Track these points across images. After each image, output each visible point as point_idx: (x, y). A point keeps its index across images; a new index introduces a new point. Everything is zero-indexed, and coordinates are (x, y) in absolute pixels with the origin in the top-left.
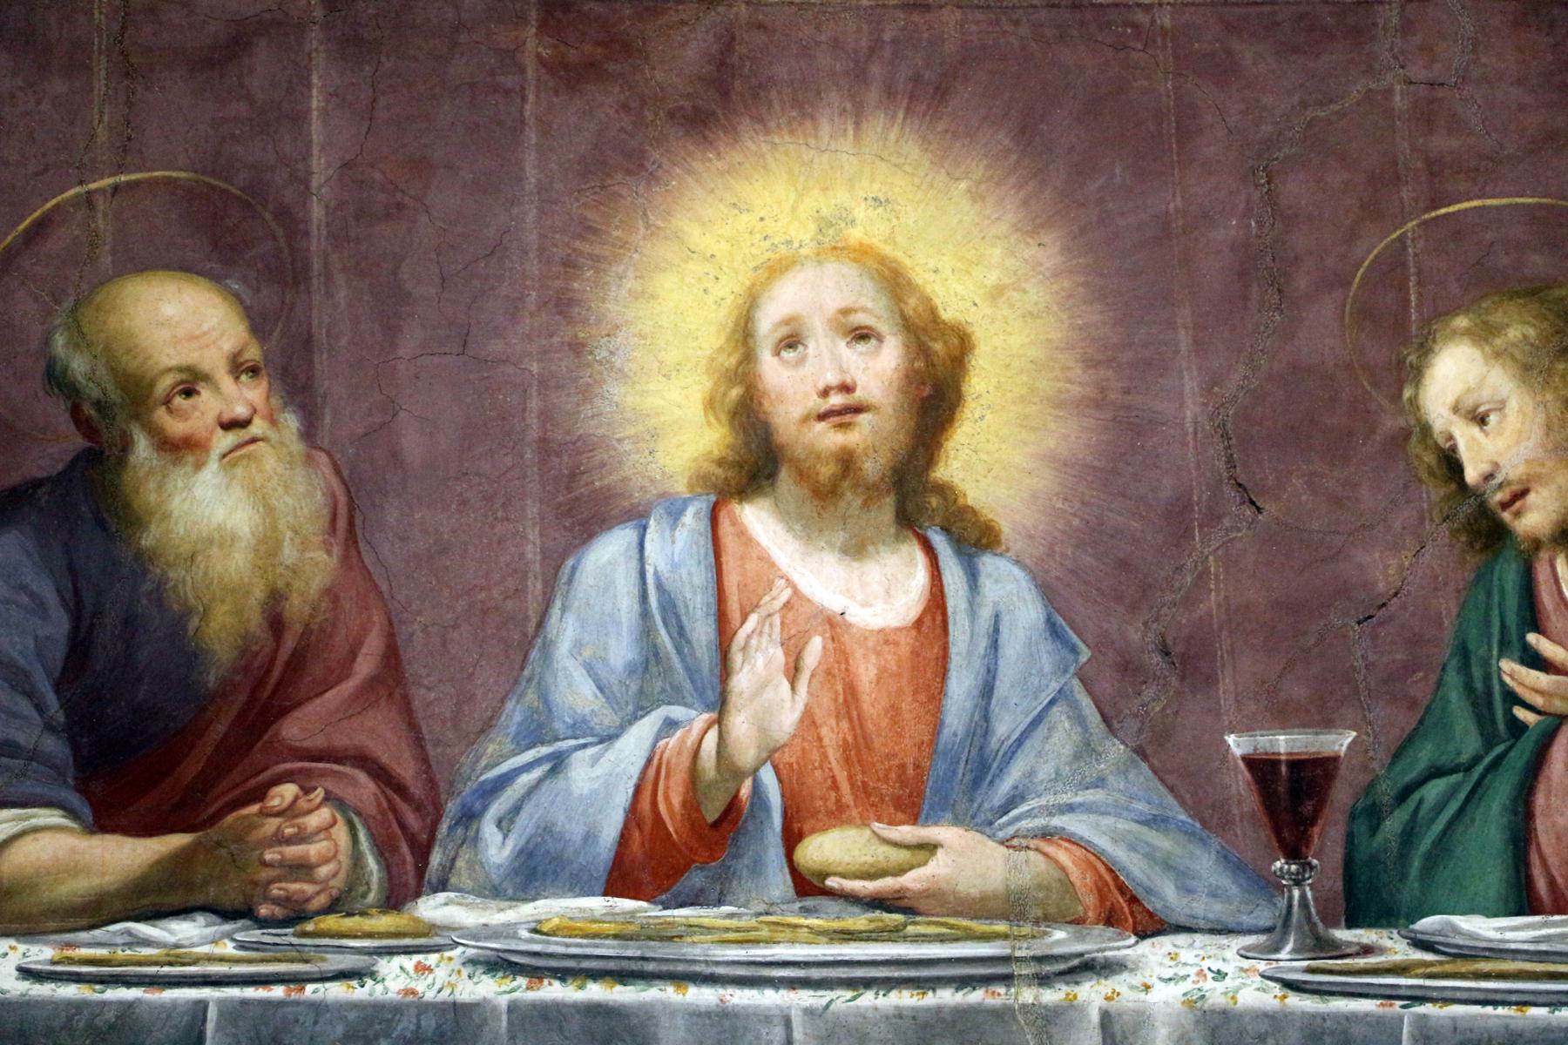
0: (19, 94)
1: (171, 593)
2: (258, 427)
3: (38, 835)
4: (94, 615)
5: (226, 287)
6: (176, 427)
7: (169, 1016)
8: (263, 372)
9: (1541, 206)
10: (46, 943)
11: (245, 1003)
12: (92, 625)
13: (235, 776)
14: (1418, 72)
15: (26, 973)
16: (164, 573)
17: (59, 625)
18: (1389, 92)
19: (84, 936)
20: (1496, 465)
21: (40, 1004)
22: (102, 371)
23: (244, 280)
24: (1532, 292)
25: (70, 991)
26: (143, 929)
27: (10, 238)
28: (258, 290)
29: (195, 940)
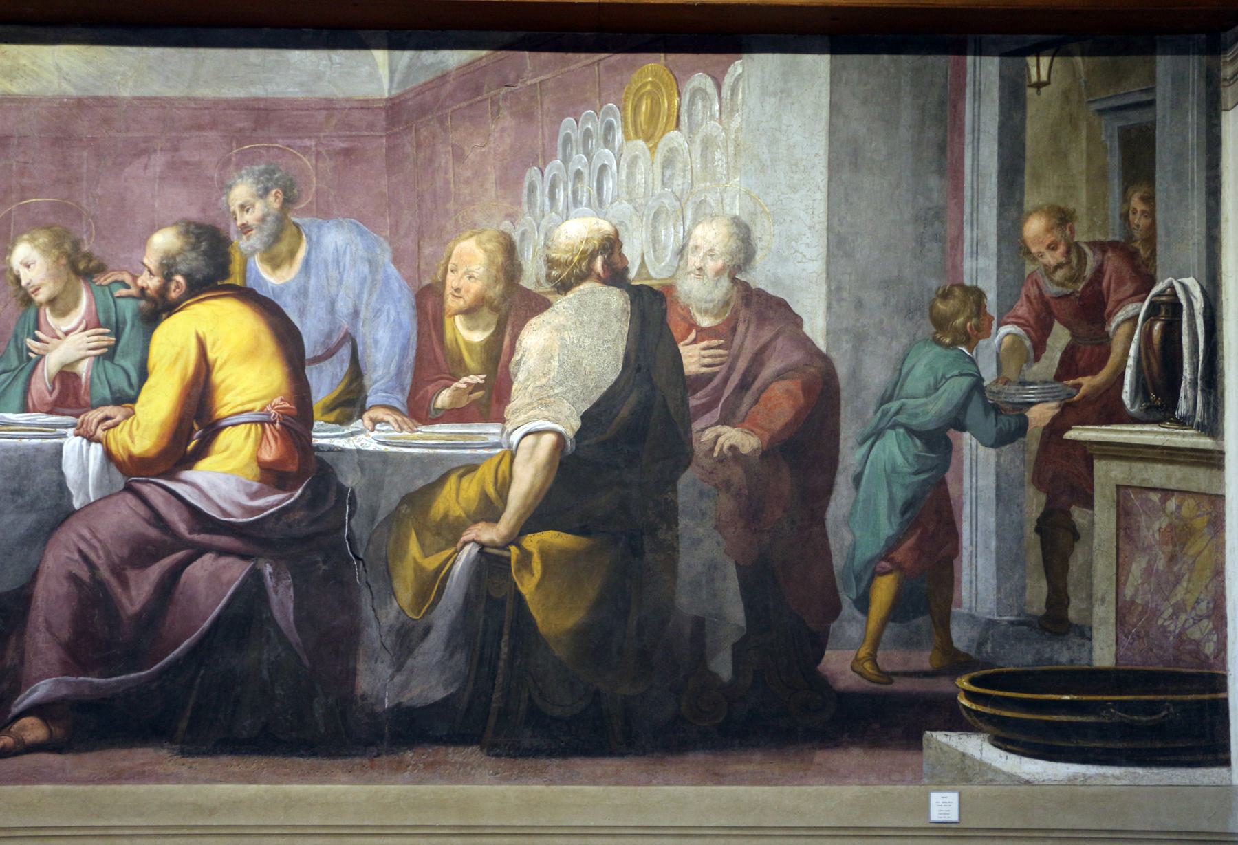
9: (54, 202)
14: (21, 158)
18: (11, 165)
20: (31, 280)
24: (48, 227)
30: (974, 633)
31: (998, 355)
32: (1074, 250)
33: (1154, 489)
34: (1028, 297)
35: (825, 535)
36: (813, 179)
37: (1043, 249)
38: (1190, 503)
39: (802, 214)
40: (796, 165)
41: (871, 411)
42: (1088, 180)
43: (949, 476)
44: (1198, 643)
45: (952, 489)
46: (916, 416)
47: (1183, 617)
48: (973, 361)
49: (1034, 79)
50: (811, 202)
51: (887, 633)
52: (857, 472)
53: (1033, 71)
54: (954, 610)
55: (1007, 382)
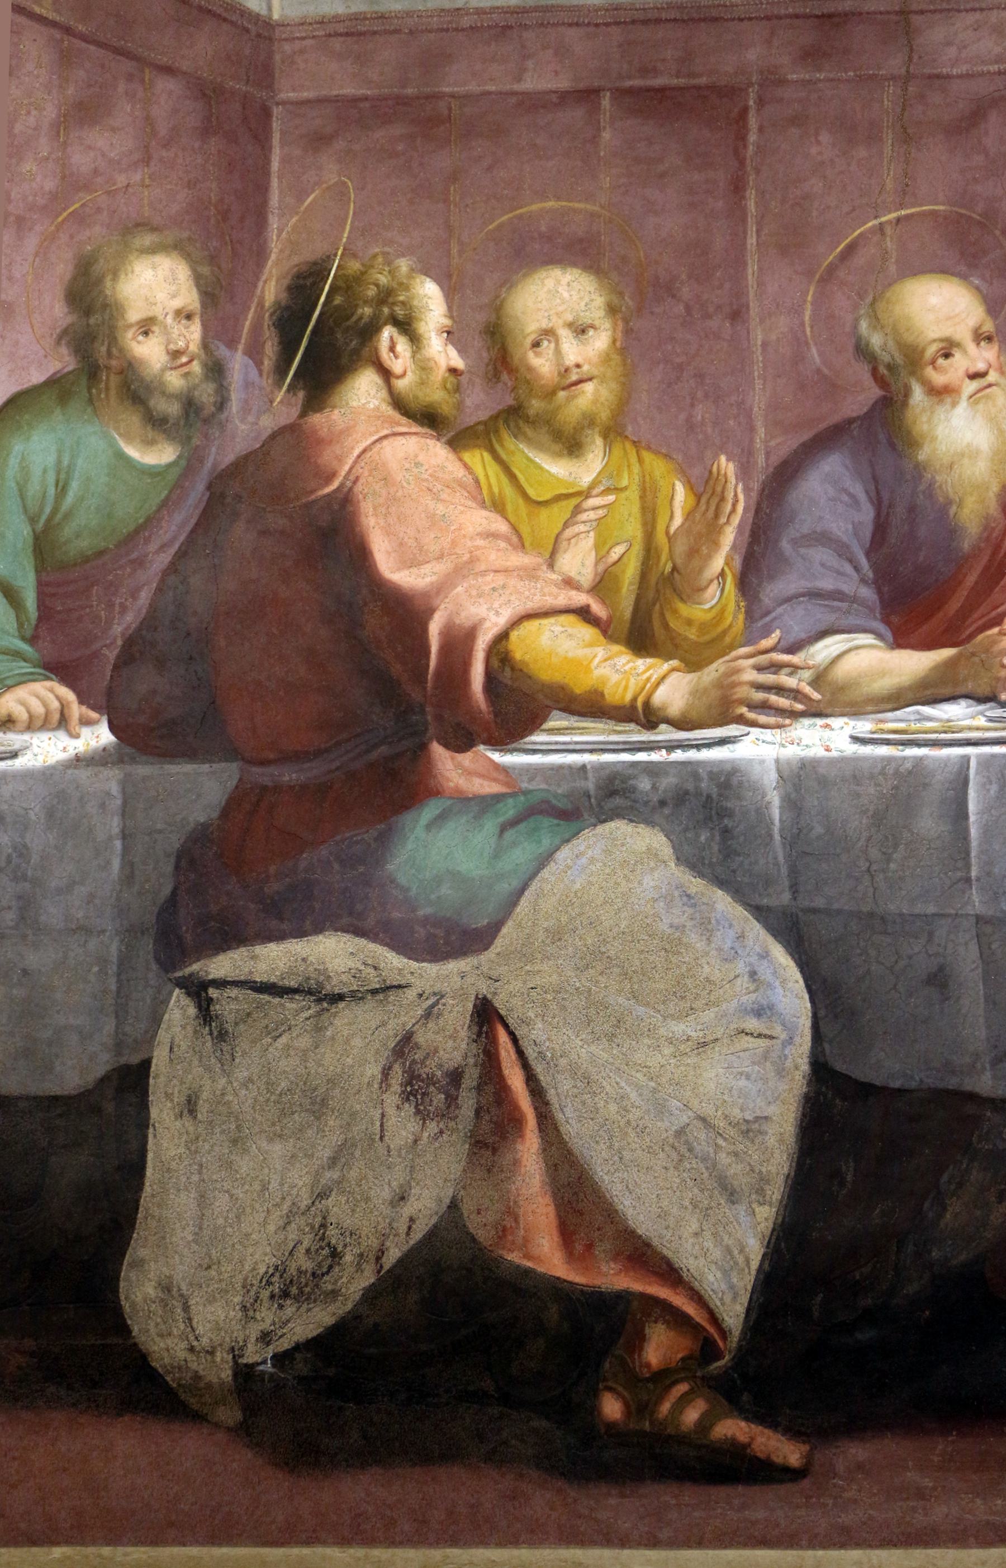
0: (837, 160)
1: (938, 491)
2: (992, 377)
3: (860, 651)
4: (890, 507)
5: (971, 283)
6: (938, 379)
7: (946, 765)
8: (996, 339)
10: (868, 720)
11: (994, 756)
12: (888, 514)
13: (982, 610)
15: (856, 739)
16: (933, 477)
17: (867, 514)
19: (889, 715)
21: (865, 759)
22: (891, 343)
23: (983, 278)
25: (883, 751)
26: (927, 710)
27: (831, 258)
28: (991, 284)
29: (960, 717)
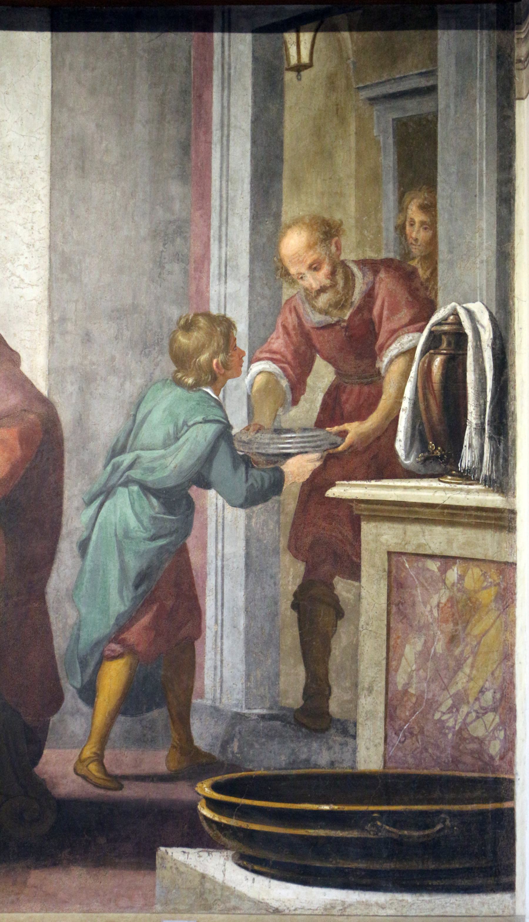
30: (220, 729)
31: (249, 397)
32: (340, 270)
33: (432, 557)
34: (284, 327)
35: (45, 614)
36: (32, 186)
37: (303, 269)
38: (475, 572)
39: (19, 229)
40: (12, 169)
41: (100, 465)
42: (357, 186)
43: (191, 542)
44: (481, 741)
45: (194, 558)
46: (152, 470)
47: (465, 709)
48: (220, 405)
49: (294, 61)
50: (30, 215)
51: (116, 729)
52: (84, 537)
53: (293, 50)
54: (196, 701)
55: (259, 429)
